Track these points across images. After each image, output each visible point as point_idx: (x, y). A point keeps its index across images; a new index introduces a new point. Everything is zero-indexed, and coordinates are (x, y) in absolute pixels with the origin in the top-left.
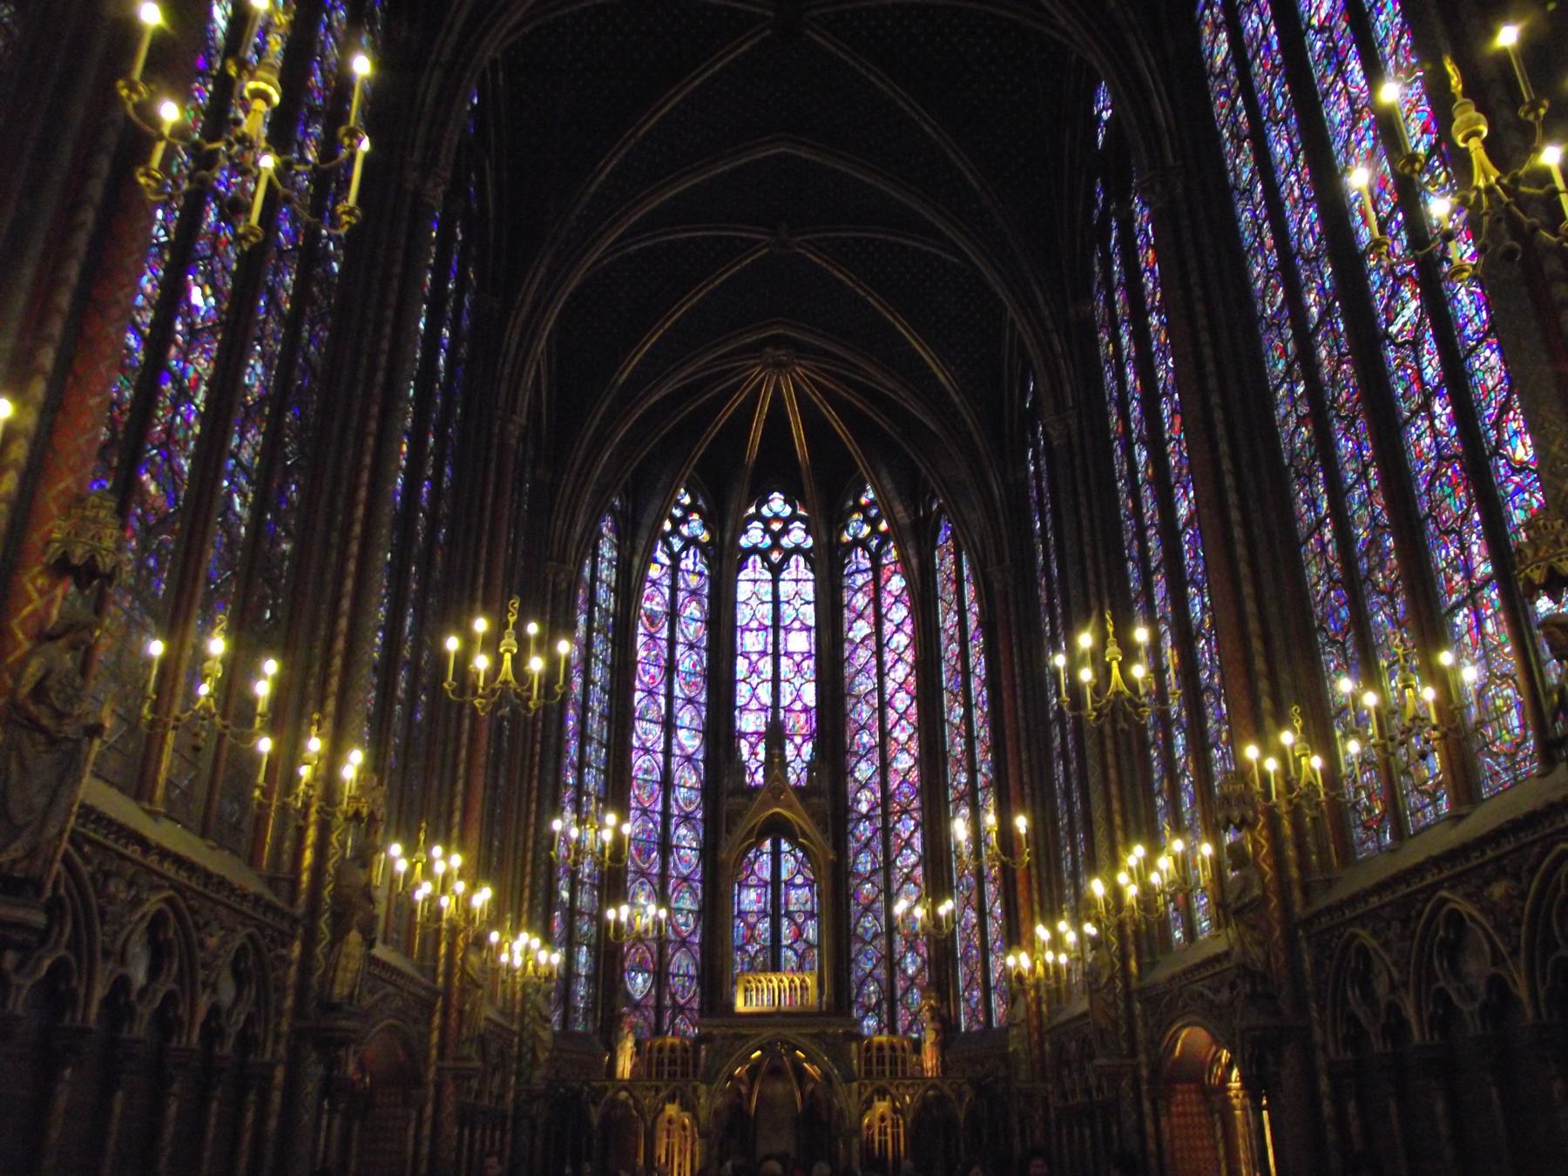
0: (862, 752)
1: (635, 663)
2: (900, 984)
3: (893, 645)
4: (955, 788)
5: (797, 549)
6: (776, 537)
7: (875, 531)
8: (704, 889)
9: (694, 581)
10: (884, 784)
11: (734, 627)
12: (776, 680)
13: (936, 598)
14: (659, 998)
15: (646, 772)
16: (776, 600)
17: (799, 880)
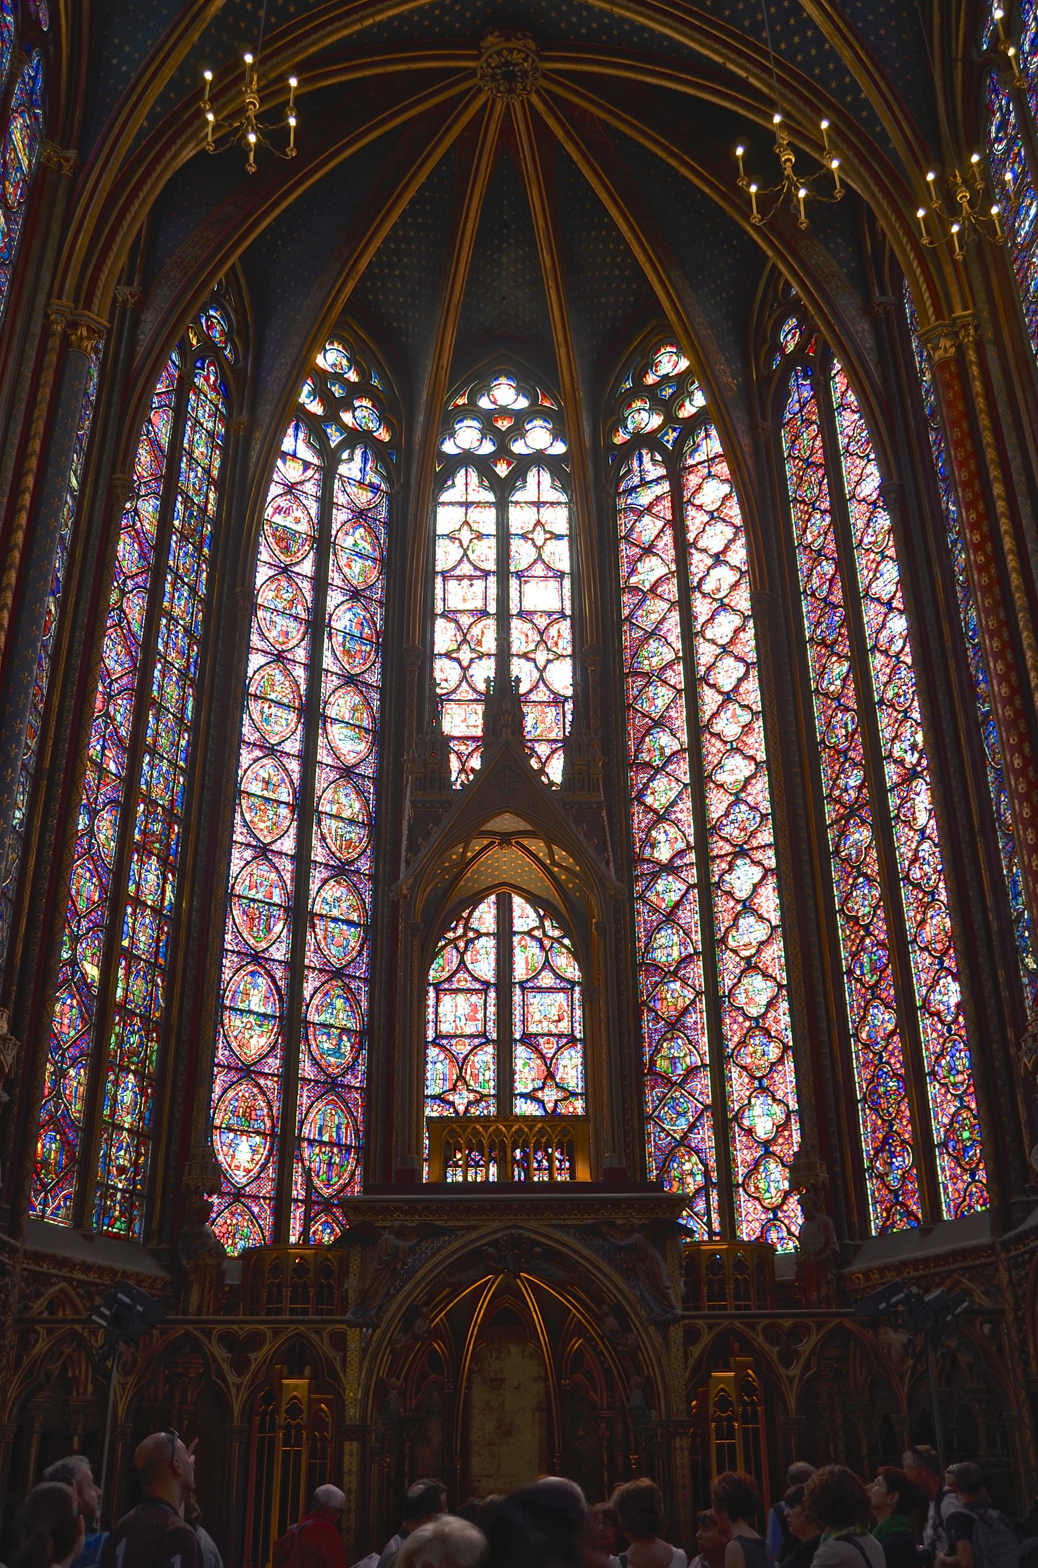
0: (657, 762)
1: (254, 607)
2: (743, 1155)
3: (707, 588)
4: (838, 801)
5: (539, 459)
7: (671, 419)
8: (371, 994)
9: (363, 497)
10: (700, 809)
11: (430, 574)
12: (503, 655)
13: (785, 501)
14: (283, 1184)
15: (267, 783)
16: (503, 546)
17: (547, 979)
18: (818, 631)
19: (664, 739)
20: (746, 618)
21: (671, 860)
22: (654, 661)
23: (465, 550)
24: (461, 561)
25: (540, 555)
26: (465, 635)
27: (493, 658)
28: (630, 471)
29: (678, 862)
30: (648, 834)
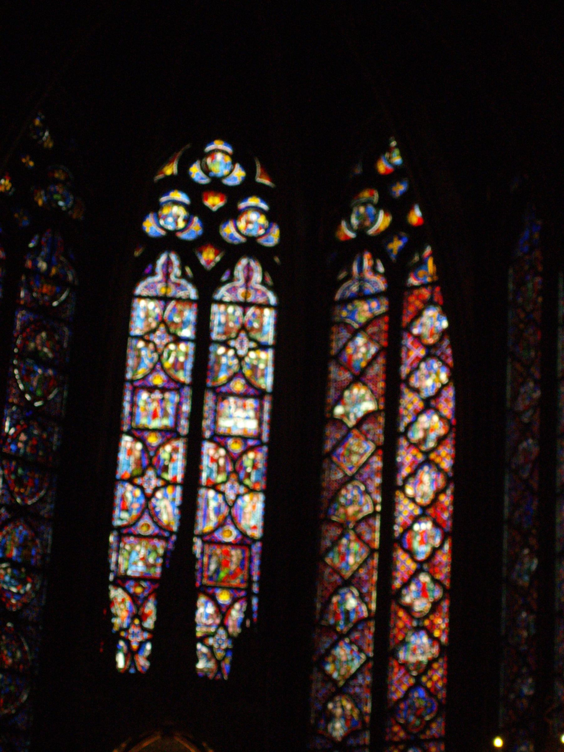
0: (341, 626)
3: (417, 435)
5: (251, 247)
6: (212, 222)
7: (399, 225)
10: (380, 688)
12: (191, 484)
18: (517, 515)
19: (352, 603)
20: (448, 480)
21: (345, 738)
22: (351, 510)
23: (160, 356)
24: (153, 370)
25: (241, 368)
26: (151, 458)
27: (179, 490)
28: (350, 276)
29: (352, 742)
30: (325, 706)
